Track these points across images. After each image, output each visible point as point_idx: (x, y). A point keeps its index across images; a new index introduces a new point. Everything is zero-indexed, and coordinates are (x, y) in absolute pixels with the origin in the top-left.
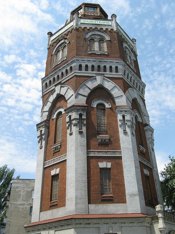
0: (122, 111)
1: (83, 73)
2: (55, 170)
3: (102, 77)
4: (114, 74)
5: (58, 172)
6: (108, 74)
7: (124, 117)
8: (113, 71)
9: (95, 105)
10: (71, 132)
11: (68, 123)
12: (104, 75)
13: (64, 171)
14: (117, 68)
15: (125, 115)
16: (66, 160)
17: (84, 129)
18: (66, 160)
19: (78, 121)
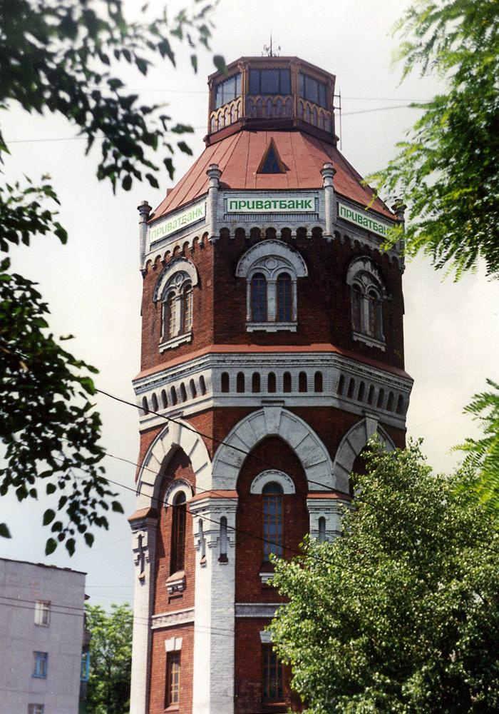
0: (319, 509)
1: (233, 399)
2: (173, 639)
3: (281, 409)
4: (310, 400)
5: (178, 648)
6: (297, 399)
7: (322, 521)
8: (308, 388)
9: (257, 487)
10: (204, 560)
11: (196, 535)
12: (282, 405)
13: (189, 642)
14: (318, 377)
15: (326, 517)
16: (192, 624)
17: (231, 555)
18: (192, 624)
19: (218, 535)
